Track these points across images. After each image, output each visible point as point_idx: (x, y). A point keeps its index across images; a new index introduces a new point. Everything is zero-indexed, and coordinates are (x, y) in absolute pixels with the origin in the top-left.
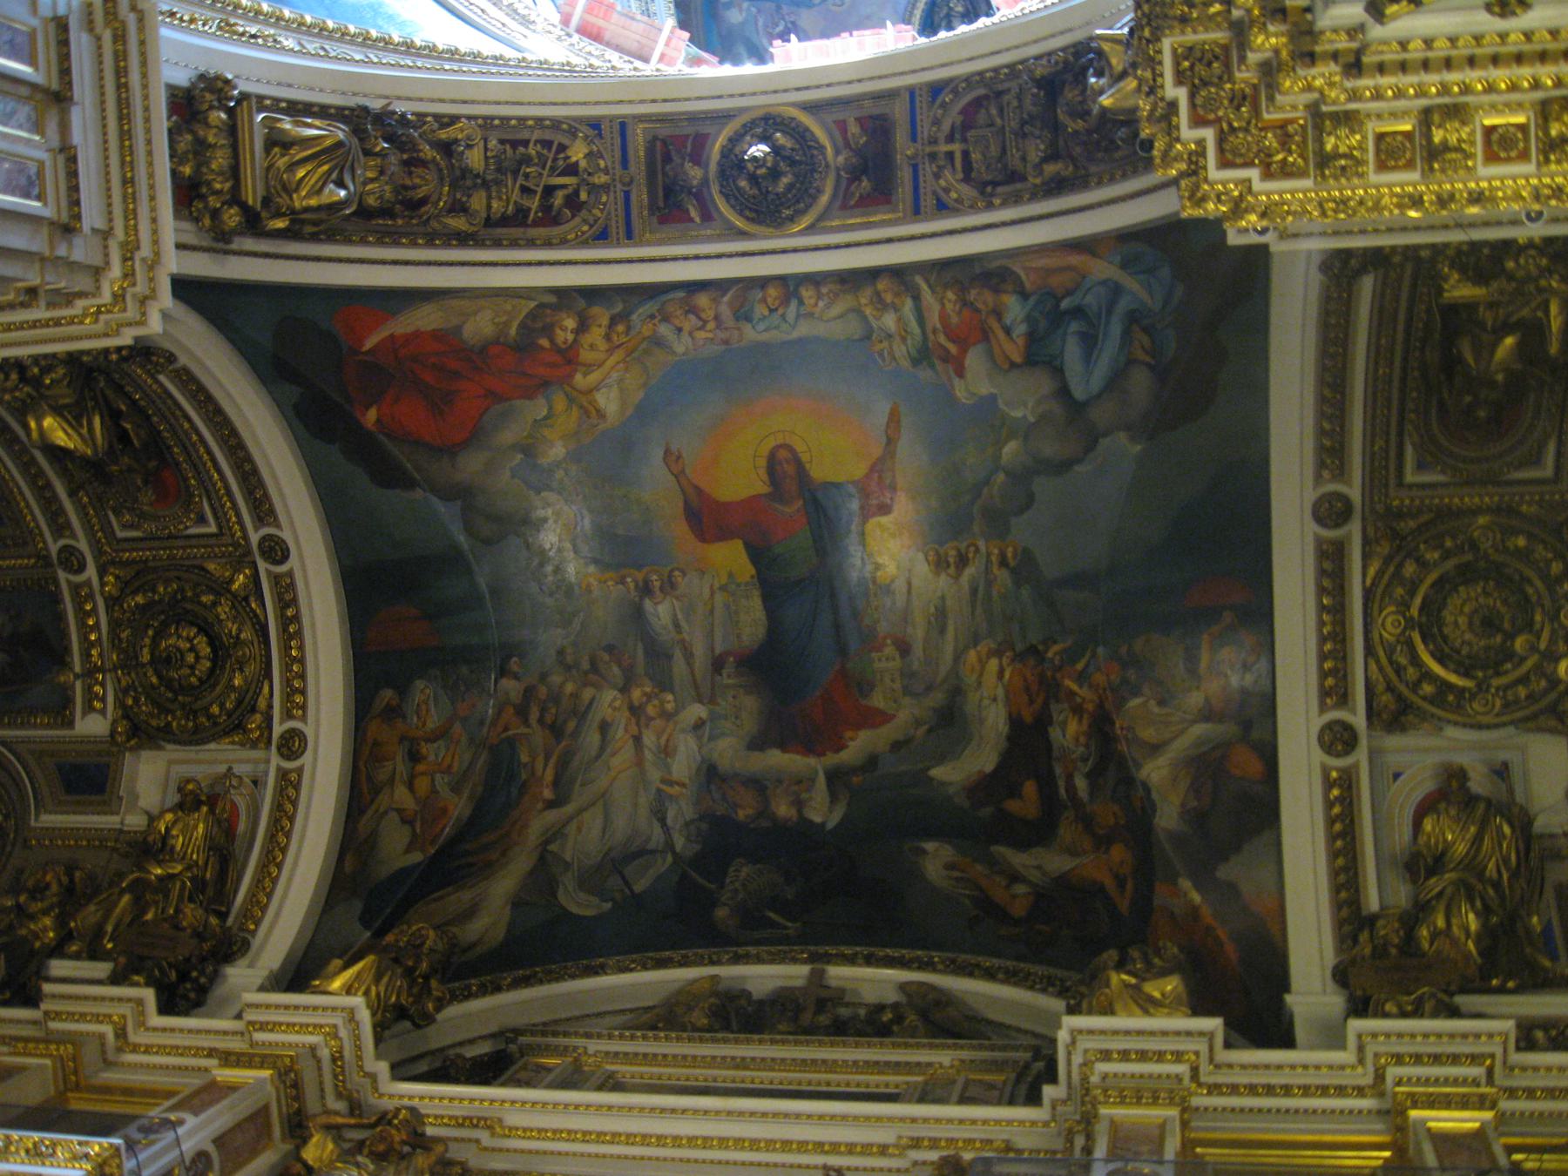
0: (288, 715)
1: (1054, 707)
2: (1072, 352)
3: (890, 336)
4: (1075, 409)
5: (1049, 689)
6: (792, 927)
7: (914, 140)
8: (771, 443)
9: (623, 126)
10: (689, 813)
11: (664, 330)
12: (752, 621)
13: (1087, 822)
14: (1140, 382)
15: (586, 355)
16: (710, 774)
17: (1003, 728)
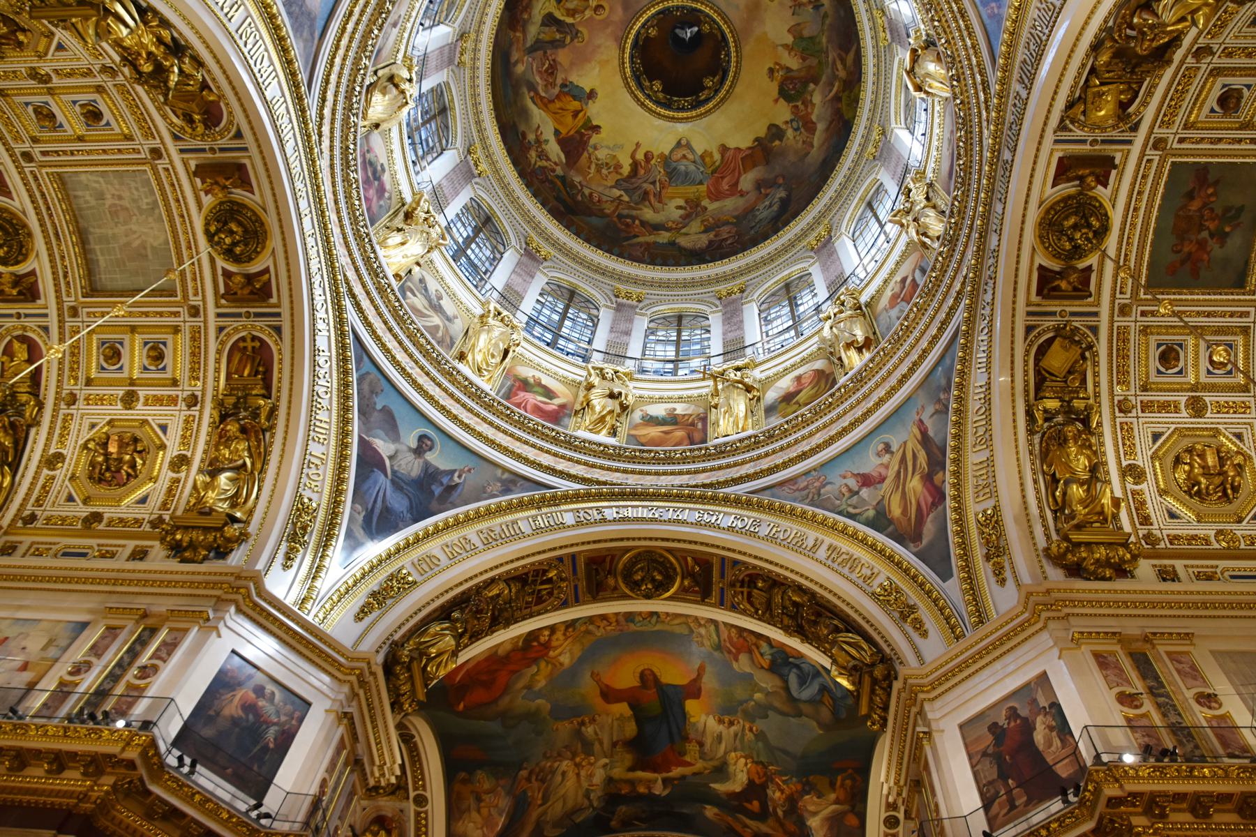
0: (416, 789)
2: (793, 679)
3: (702, 636)
4: (792, 700)
5: (769, 778)
6: (644, 826)
7: (722, 576)
8: (642, 668)
9: (573, 557)
10: (600, 793)
11: (591, 627)
12: (631, 729)
13: (782, 825)
14: (825, 713)
15: (554, 643)
16: (610, 780)
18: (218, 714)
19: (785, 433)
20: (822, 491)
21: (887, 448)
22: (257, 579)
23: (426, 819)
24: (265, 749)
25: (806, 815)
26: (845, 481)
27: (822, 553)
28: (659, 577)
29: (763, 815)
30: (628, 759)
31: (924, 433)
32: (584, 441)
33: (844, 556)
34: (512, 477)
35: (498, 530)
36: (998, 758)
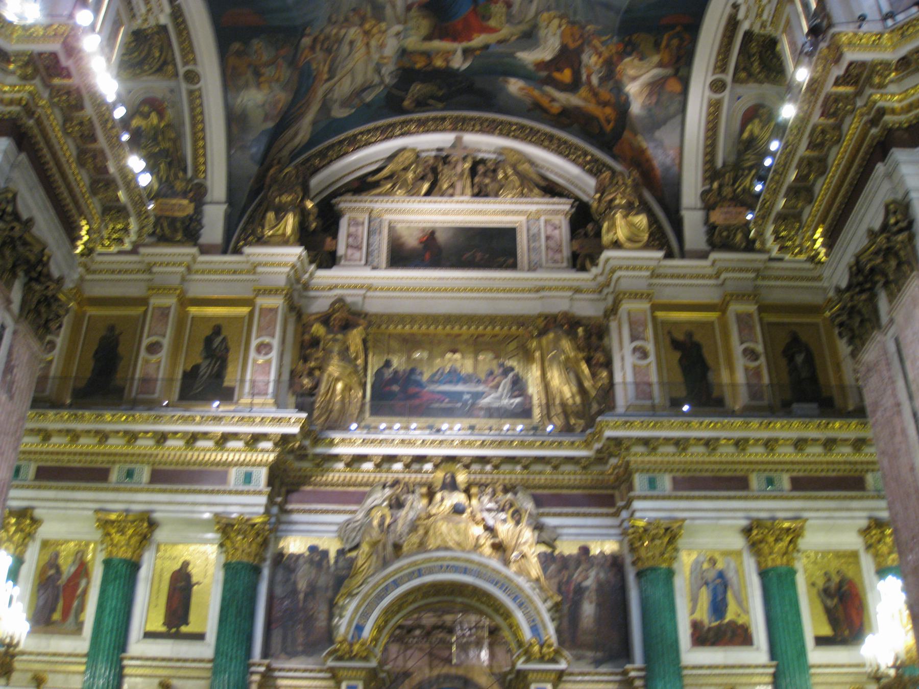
0: (186, 63)
1: (586, 46)
5: (585, 41)
6: (440, 105)
13: (595, 94)
16: (403, 52)
23: (200, 97)
25: (625, 79)
29: (574, 86)
30: (425, 25)
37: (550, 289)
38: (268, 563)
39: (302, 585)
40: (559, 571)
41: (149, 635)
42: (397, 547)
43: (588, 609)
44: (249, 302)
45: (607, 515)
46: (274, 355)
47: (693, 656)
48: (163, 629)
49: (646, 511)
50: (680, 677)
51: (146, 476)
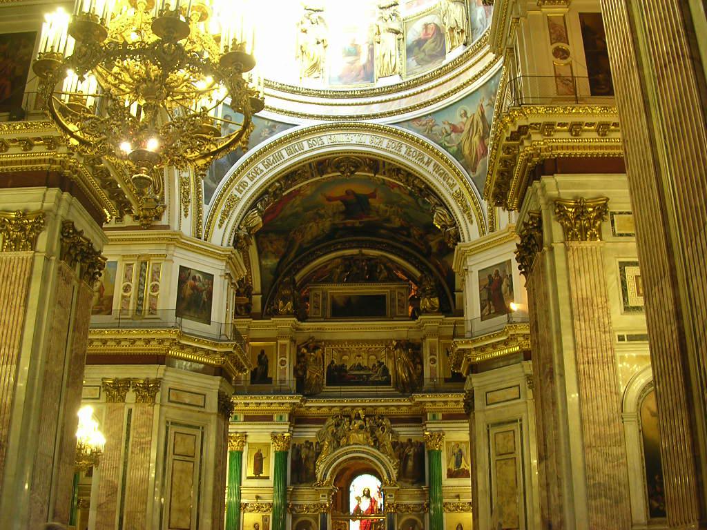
2: (420, 201)
7: (384, 166)
9: (310, 164)
12: (343, 208)
17: (399, 224)
18: (184, 296)
19: (416, 85)
20: (434, 128)
21: (465, 113)
22: (181, 235)
24: (204, 302)
26: (444, 126)
27: (431, 168)
28: (353, 169)
30: (342, 217)
31: (483, 113)
32: (306, 89)
33: (442, 171)
34: (273, 123)
35: (272, 158)
36: (489, 290)
37: (399, 327)
38: (291, 448)
39: (303, 456)
40: (400, 449)
41: (248, 478)
42: (339, 443)
43: (410, 463)
44: (275, 340)
45: (419, 427)
46: (287, 364)
47: (447, 482)
48: (254, 476)
49: (432, 427)
50: (441, 491)
51: (242, 419)
